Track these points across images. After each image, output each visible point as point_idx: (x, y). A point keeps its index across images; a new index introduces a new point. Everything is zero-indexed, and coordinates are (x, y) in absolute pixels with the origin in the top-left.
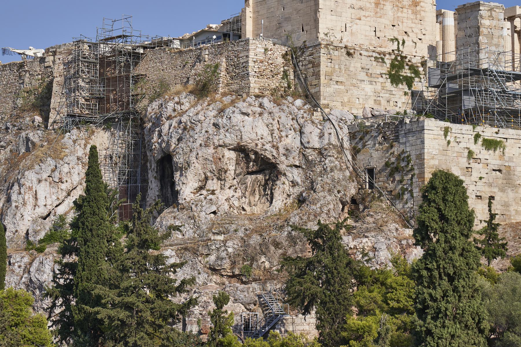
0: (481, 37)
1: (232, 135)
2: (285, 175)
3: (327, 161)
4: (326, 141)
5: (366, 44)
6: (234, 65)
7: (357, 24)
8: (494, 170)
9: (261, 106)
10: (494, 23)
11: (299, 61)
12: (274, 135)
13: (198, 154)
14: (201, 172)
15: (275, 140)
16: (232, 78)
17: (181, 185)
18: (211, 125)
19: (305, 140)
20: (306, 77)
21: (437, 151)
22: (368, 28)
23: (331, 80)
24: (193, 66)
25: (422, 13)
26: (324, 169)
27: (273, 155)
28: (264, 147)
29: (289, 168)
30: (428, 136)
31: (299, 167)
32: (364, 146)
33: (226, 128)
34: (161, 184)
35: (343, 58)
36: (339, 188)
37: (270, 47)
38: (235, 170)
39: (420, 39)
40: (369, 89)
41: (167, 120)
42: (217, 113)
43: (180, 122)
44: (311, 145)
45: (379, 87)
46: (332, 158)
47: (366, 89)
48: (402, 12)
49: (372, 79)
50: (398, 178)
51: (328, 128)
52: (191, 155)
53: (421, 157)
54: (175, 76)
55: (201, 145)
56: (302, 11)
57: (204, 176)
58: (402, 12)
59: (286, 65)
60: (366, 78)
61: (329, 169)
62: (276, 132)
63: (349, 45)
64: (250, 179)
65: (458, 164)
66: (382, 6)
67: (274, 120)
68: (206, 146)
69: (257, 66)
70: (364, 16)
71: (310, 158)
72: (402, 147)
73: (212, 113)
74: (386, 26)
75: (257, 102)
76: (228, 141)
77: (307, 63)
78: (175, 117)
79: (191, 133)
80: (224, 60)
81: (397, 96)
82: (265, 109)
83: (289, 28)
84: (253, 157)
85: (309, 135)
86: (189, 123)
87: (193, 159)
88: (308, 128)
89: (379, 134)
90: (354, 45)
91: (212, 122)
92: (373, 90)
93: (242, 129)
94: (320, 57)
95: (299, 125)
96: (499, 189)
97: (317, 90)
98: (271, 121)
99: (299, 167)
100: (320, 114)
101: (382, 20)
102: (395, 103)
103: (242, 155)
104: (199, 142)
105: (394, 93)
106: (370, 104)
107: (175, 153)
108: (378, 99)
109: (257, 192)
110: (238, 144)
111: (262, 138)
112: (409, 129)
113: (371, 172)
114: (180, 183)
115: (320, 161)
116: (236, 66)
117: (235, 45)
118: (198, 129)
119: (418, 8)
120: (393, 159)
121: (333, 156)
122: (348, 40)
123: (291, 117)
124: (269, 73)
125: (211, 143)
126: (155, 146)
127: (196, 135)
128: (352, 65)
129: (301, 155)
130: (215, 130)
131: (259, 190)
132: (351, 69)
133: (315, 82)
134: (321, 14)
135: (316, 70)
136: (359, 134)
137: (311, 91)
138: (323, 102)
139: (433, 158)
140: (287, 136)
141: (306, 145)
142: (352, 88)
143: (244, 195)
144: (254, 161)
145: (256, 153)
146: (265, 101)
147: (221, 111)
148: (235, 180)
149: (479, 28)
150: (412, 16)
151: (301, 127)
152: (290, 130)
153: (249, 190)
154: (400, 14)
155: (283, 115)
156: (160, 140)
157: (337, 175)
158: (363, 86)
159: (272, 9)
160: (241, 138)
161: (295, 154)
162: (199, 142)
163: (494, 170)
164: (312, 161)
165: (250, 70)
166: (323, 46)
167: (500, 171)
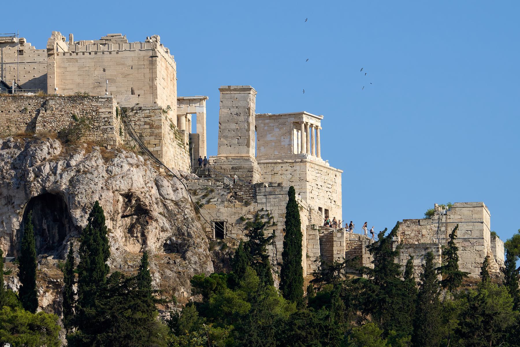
2: (156, 220)
13: (101, 196)
19: (164, 192)
26: (184, 219)
32: (208, 202)
55: (102, 188)
77: (143, 123)
79: (89, 176)
85: (167, 188)
93: (133, 177)
97: (157, 148)
104: (100, 185)
110: (129, 190)
125: (111, 187)
137: (149, 149)
145: (138, 199)
159: (87, 69)
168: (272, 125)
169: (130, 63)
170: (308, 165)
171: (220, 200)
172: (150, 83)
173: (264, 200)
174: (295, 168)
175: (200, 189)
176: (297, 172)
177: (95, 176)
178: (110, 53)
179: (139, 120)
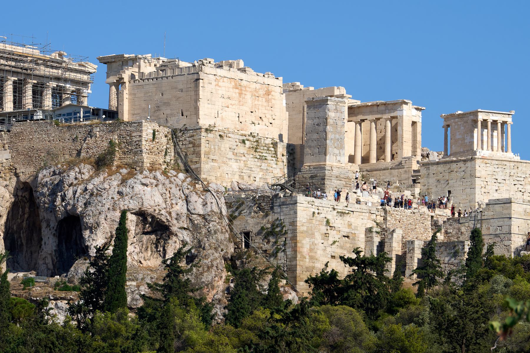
0: (328, 127)
1: (135, 202)
2: (176, 235)
3: (211, 225)
4: (209, 209)
5: (232, 128)
6: (127, 142)
8: (344, 236)
9: (155, 178)
10: (338, 114)
11: (179, 141)
12: (167, 203)
13: (107, 216)
14: (108, 230)
15: (168, 207)
16: (125, 154)
17: (91, 241)
18: (116, 192)
19: (191, 208)
20: (186, 155)
24: (85, 140)
25: (273, 100)
26: (208, 232)
27: (167, 219)
28: (161, 212)
29: (180, 230)
30: (300, 208)
31: (187, 229)
32: (240, 214)
33: (130, 196)
34: (59, 240)
35: (217, 140)
36: (222, 247)
38: (135, 230)
39: (271, 123)
40: (235, 166)
41: (69, 186)
42: (120, 183)
43: (86, 189)
44: (197, 212)
45: (242, 164)
46: (215, 223)
48: (258, 100)
50: (272, 240)
51: (209, 198)
52: (100, 217)
53: (293, 223)
54: (64, 147)
55: (109, 209)
56: (181, 99)
57: (110, 234)
58: (258, 100)
59: (168, 143)
60: (233, 157)
61: (213, 232)
62: (168, 199)
64: (145, 238)
65: (319, 230)
67: (166, 190)
68: (114, 210)
69: (147, 145)
70: (231, 104)
71: (196, 222)
72: (276, 216)
73: (115, 183)
75: (151, 175)
76: (131, 206)
77: (188, 143)
78: (80, 184)
79: (99, 198)
80: (116, 137)
81: (255, 172)
82: (158, 181)
83: (168, 112)
84: (150, 220)
85: (195, 203)
86: (95, 190)
87: (102, 220)
88: (194, 198)
89: (255, 205)
91: (117, 190)
92: (238, 167)
93: (143, 196)
94: (200, 139)
95: (184, 195)
96: (348, 251)
97: (197, 166)
98: (165, 191)
99: (187, 229)
100: (201, 186)
102: (254, 179)
103: (141, 218)
104: (107, 206)
105: (253, 169)
106: (236, 179)
107: (85, 215)
108: (242, 174)
109: (149, 249)
110: (140, 209)
111: (159, 205)
112: (283, 202)
113: (247, 234)
114: (91, 239)
115: (204, 225)
116: (129, 143)
117: (127, 126)
118: (105, 196)
119: (270, 97)
120: (269, 226)
121: (215, 221)
122: (220, 125)
123: (178, 188)
124: (157, 151)
126: (59, 208)
127: (104, 201)
128: (223, 146)
129: (188, 220)
130: (119, 197)
131: (151, 247)
132: (222, 149)
133: (195, 159)
134: (200, 103)
135: (197, 149)
136: (236, 204)
137: (191, 166)
138: (203, 176)
139: (303, 226)
140: (177, 204)
141: (193, 211)
142: (223, 165)
143: (141, 251)
144: (151, 224)
145: (153, 217)
146: (158, 174)
147: (124, 181)
148: (135, 239)
149: (326, 119)
150: (265, 104)
151: (187, 197)
152: (180, 199)
153: (144, 246)
154: (256, 102)
155: (173, 186)
156: (64, 204)
157: (220, 237)
158: (231, 163)
159: (150, 94)
160: (142, 204)
161: (184, 218)
162: (107, 206)
163: (344, 236)
164: (197, 225)
165: (143, 148)
166: (203, 130)
167: (348, 237)
168: (459, 123)
169: (181, 86)
170: (478, 162)
171: (248, 211)
172: (195, 104)
173: (279, 210)
174: (467, 165)
175: (234, 202)
176: (469, 169)
177: (103, 198)
178: (167, 78)
179: (185, 139)
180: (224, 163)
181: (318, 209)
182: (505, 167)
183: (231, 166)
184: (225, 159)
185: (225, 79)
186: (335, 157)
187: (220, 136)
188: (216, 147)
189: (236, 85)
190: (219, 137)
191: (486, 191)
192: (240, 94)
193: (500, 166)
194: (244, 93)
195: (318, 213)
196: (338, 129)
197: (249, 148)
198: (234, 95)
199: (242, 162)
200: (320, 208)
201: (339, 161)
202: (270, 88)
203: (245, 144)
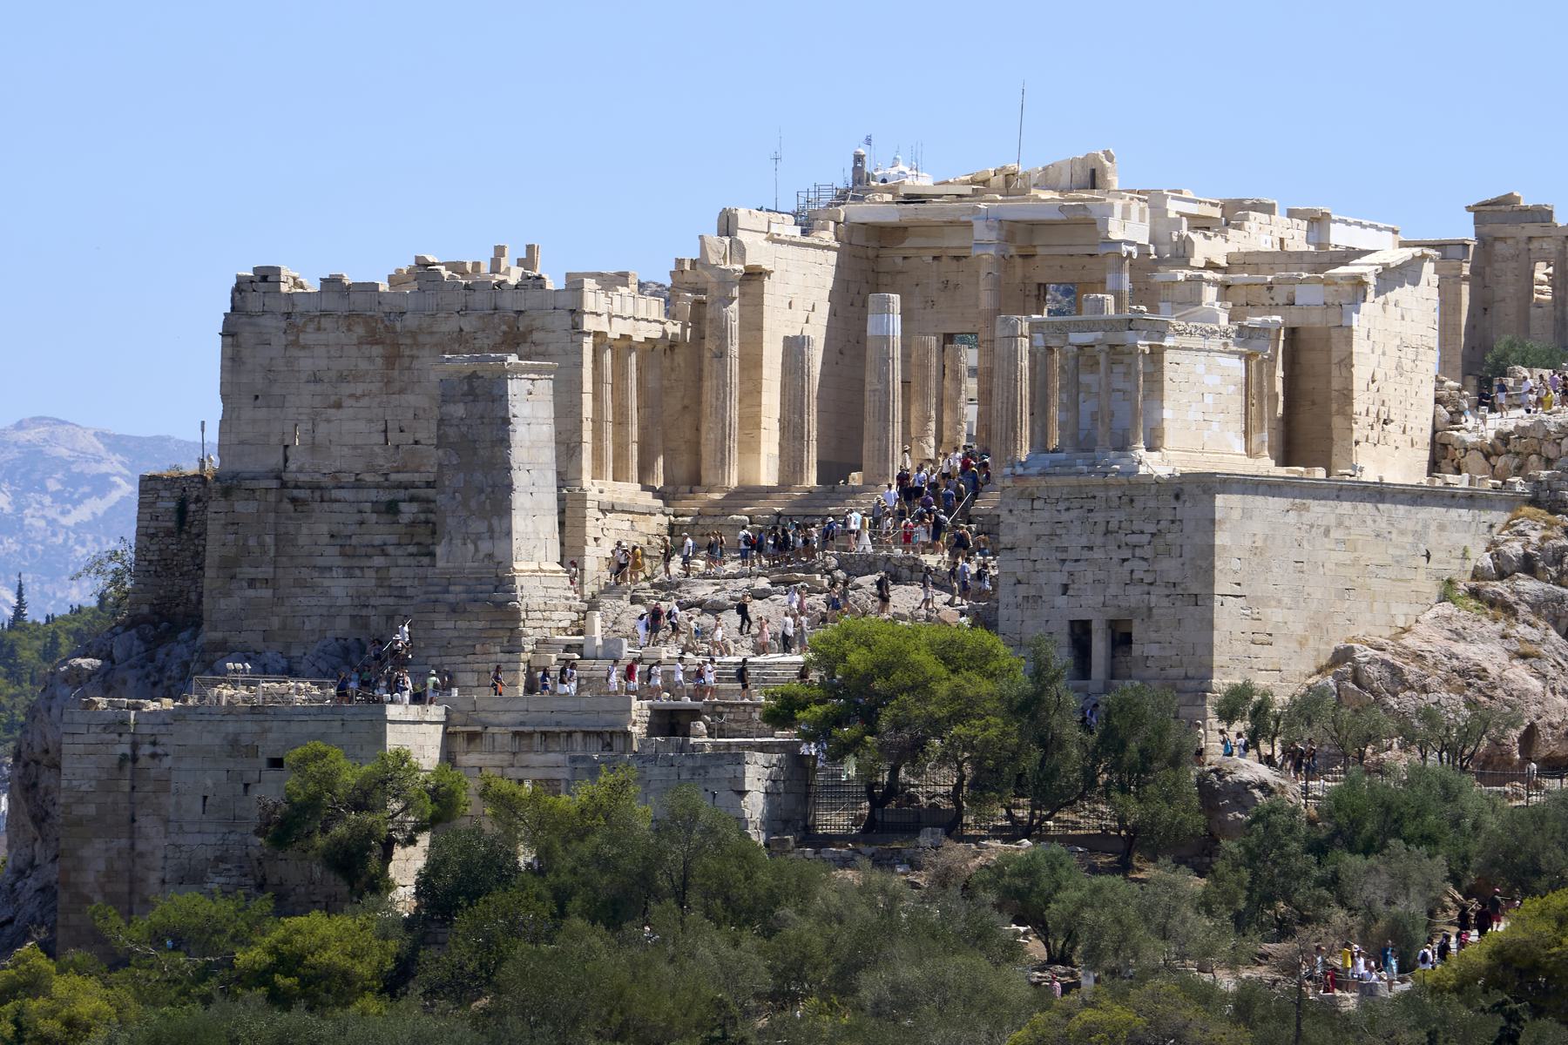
7: (328, 421)
21: (94, 783)
22: (361, 426)
23: (233, 577)
37: (195, 494)
40: (339, 588)
47: (334, 591)
49: (355, 562)
60: (339, 561)
63: (302, 478)
66: (406, 362)
70: (352, 396)
74: (420, 413)
90: (318, 476)
101: (410, 399)
105: (409, 591)
108: (364, 612)
128: (305, 530)
132: (302, 541)
142: (298, 590)
158: (327, 583)
180: (300, 583)
181: (154, 744)
182: (1089, 504)
183: (325, 593)
184: (305, 572)
185: (325, 322)
186: (471, 547)
187: (294, 500)
188: (269, 540)
189: (372, 332)
190: (290, 507)
191: (1033, 592)
192: (391, 360)
193: (1076, 504)
194: (407, 352)
195: (154, 756)
196: (482, 452)
197: (413, 524)
198: (364, 365)
199: (370, 573)
200: (160, 739)
201: (490, 556)
202: (523, 324)
203: (397, 512)
